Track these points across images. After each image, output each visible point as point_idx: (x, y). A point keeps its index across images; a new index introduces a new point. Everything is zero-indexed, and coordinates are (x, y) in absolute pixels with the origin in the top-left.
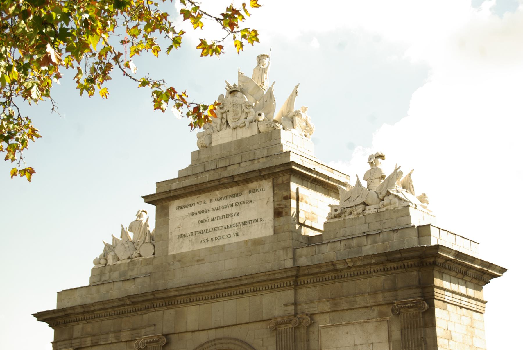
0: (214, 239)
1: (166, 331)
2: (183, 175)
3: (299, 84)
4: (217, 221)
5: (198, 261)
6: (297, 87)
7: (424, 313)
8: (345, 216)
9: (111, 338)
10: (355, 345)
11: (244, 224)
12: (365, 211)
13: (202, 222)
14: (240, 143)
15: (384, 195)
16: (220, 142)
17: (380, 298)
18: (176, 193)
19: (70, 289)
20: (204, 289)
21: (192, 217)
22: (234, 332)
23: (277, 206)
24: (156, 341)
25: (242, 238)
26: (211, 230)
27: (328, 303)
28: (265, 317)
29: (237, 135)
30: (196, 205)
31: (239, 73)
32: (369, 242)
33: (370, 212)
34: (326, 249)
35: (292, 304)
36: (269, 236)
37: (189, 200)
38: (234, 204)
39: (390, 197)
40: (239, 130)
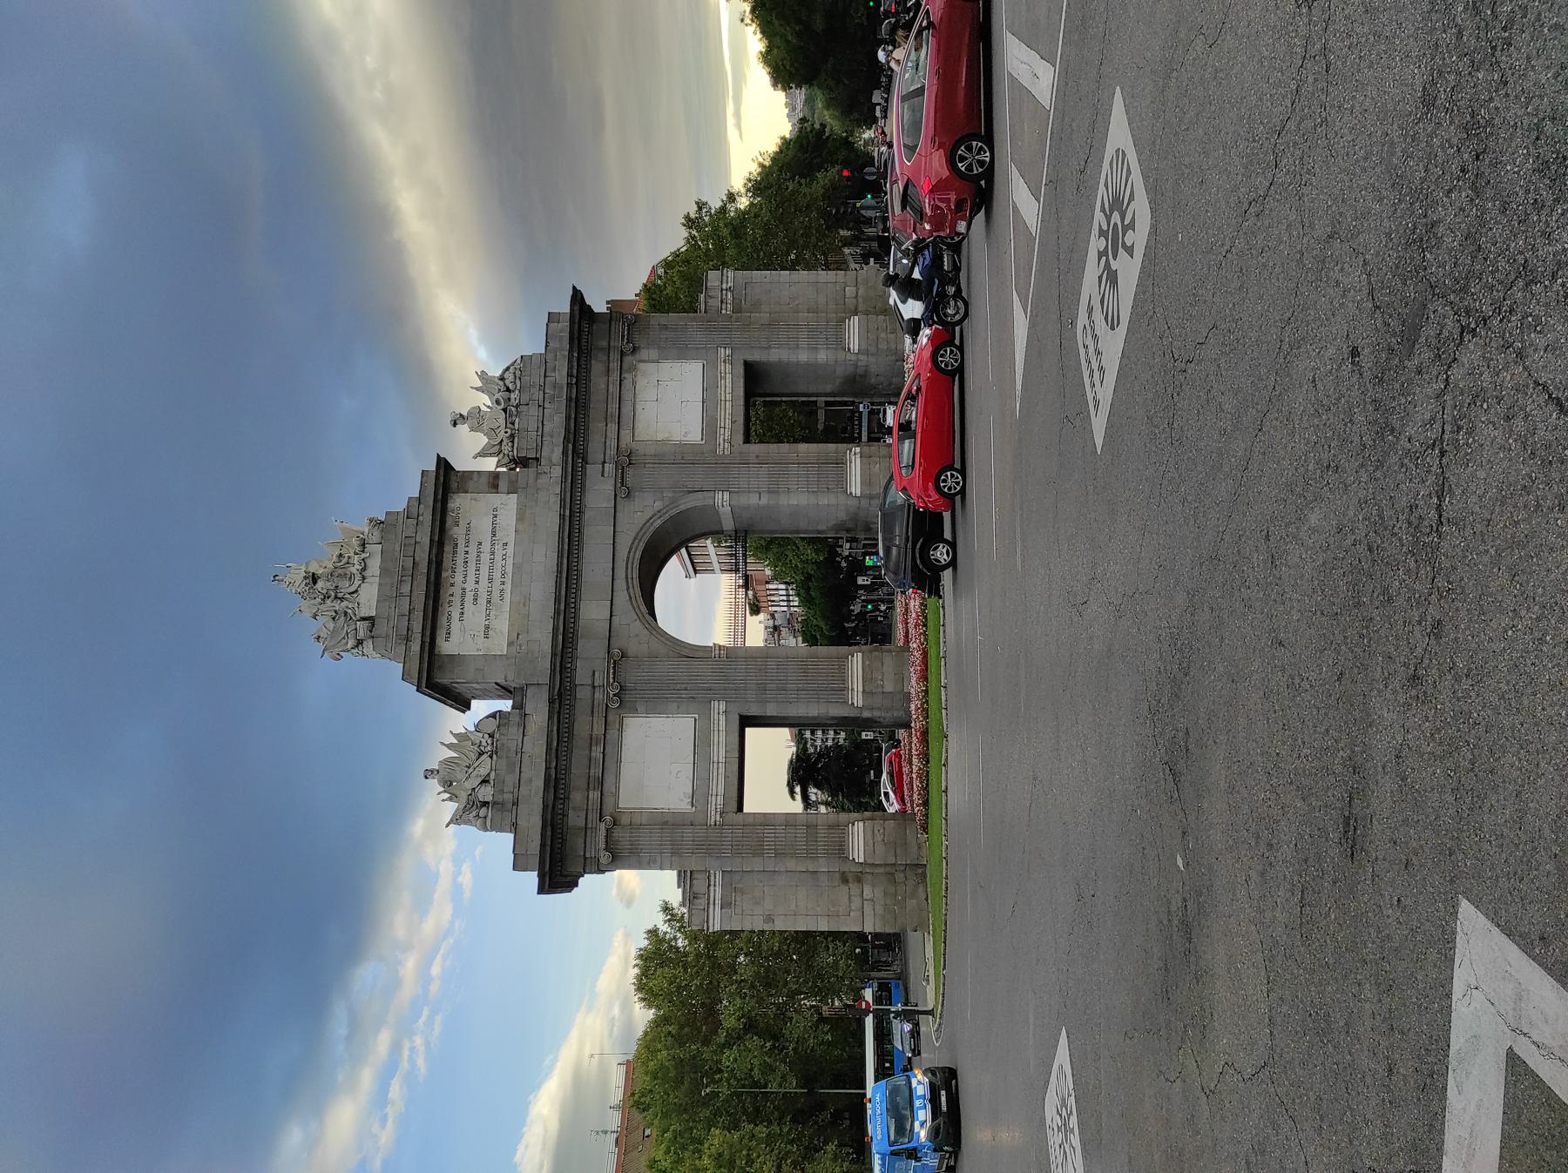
0: (502, 580)
5: (524, 605)
9: (597, 753)
14: (384, 571)
17: (615, 365)
18: (428, 633)
20: (564, 575)
24: (615, 661)
25: (511, 539)
26: (490, 585)
27: (609, 425)
32: (553, 375)
35: (603, 467)
37: (443, 621)
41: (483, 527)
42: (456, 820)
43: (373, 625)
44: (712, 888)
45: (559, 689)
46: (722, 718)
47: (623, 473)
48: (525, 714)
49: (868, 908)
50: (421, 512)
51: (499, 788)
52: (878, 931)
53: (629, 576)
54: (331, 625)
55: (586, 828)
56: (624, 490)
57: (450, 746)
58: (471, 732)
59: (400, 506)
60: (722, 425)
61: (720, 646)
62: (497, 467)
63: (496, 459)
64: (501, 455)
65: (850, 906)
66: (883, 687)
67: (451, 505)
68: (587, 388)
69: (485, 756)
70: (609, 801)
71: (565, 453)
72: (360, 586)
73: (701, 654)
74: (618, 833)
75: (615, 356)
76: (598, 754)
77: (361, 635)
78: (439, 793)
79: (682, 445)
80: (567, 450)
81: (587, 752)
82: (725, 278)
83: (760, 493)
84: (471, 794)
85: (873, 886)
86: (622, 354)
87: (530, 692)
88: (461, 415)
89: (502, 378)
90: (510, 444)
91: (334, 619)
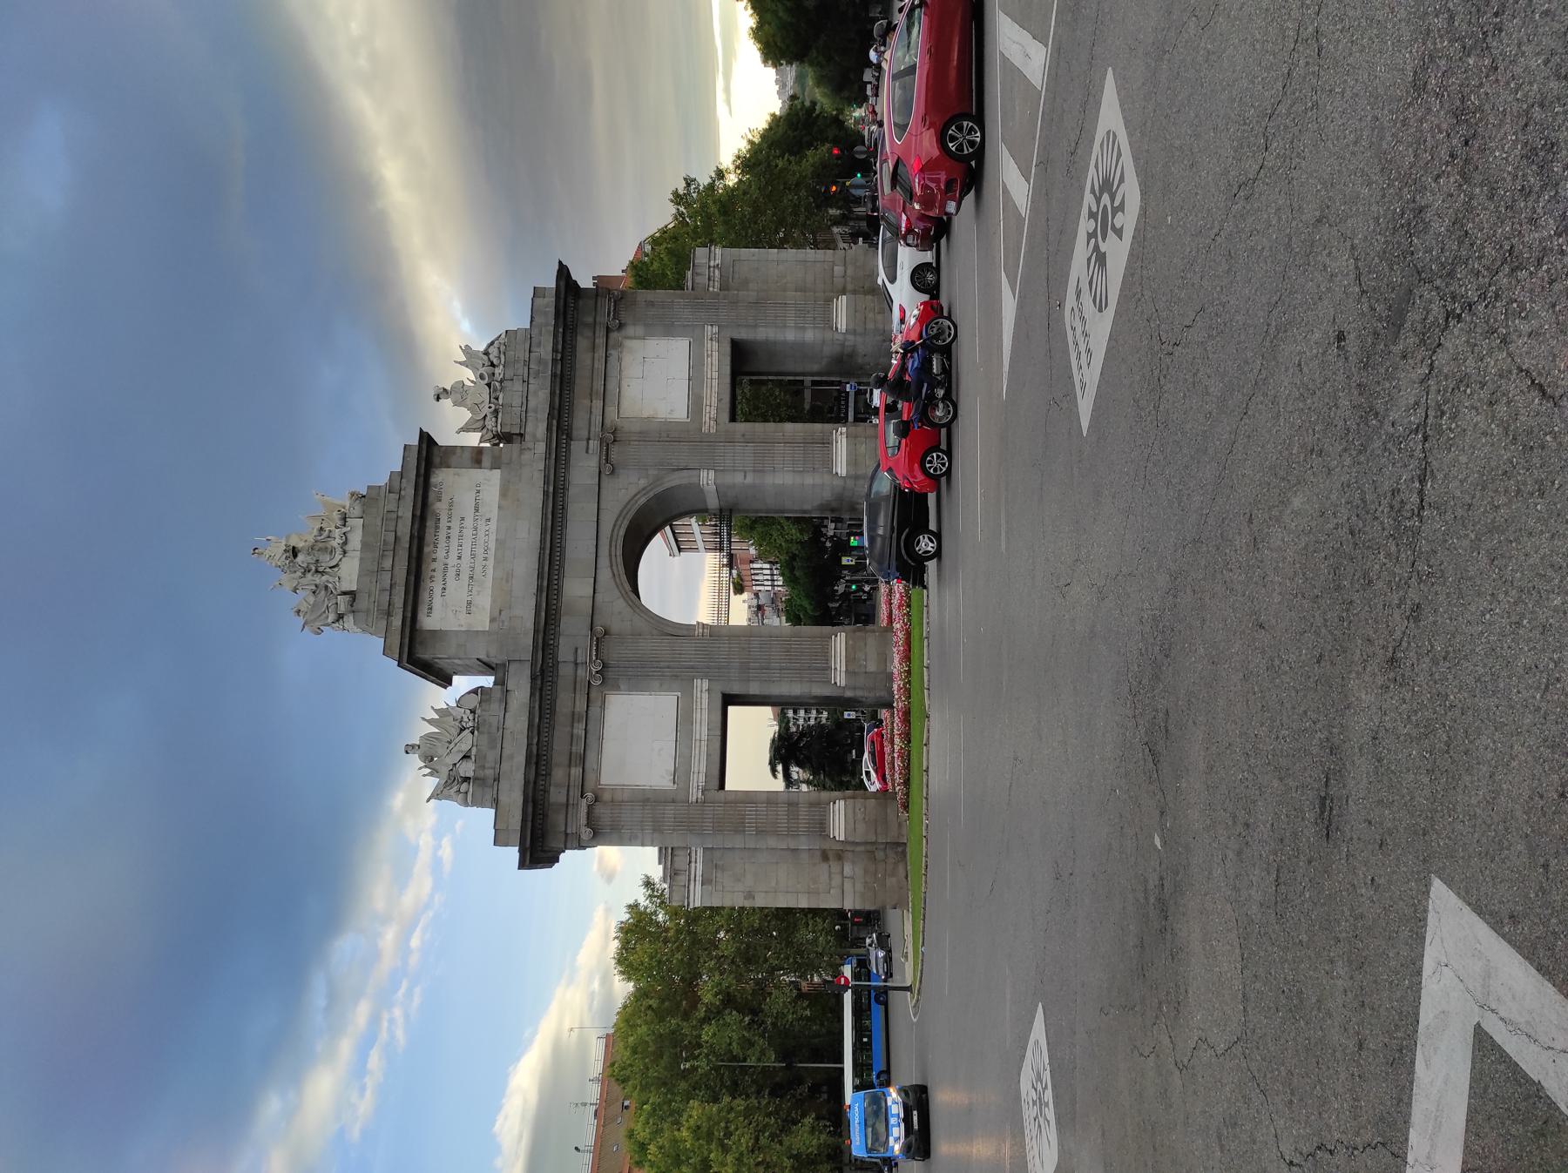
5: (507, 581)
9: (579, 730)
11: (477, 511)
14: (365, 545)
17: (600, 341)
18: (409, 608)
20: (548, 552)
24: (597, 638)
25: (494, 514)
27: (594, 401)
29: (354, 550)
34: (532, 404)
35: (588, 443)
37: (424, 596)
39: (490, 350)
41: (466, 501)
42: (437, 795)
43: (354, 600)
44: (693, 865)
45: (542, 665)
46: (705, 695)
47: (607, 449)
48: (507, 691)
49: (848, 886)
52: (858, 907)
53: (613, 554)
54: (312, 599)
55: (567, 805)
56: (608, 467)
57: (430, 722)
58: (453, 708)
59: (382, 480)
60: (708, 404)
61: (703, 624)
62: (481, 442)
63: (480, 434)
64: (485, 430)
65: (830, 884)
66: (865, 667)
67: (433, 480)
68: (573, 368)
69: (467, 731)
70: (590, 777)
71: (549, 428)
72: (340, 560)
73: (685, 633)
74: (599, 810)
75: (601, 333)
76: (580, 732)
77: (342, 609)
78: (420, 768)
79: (666, 423)
80: (552, 425)
81: (569, 729)
82: (712, 255)
83: (745, 472)
84: (452, 770)
85: (853, 863)
86: (608, 330)
87: (513, 668)
88: (445, 390)
89: (486, 353)
90: (494, 419)
91: (314, 592)
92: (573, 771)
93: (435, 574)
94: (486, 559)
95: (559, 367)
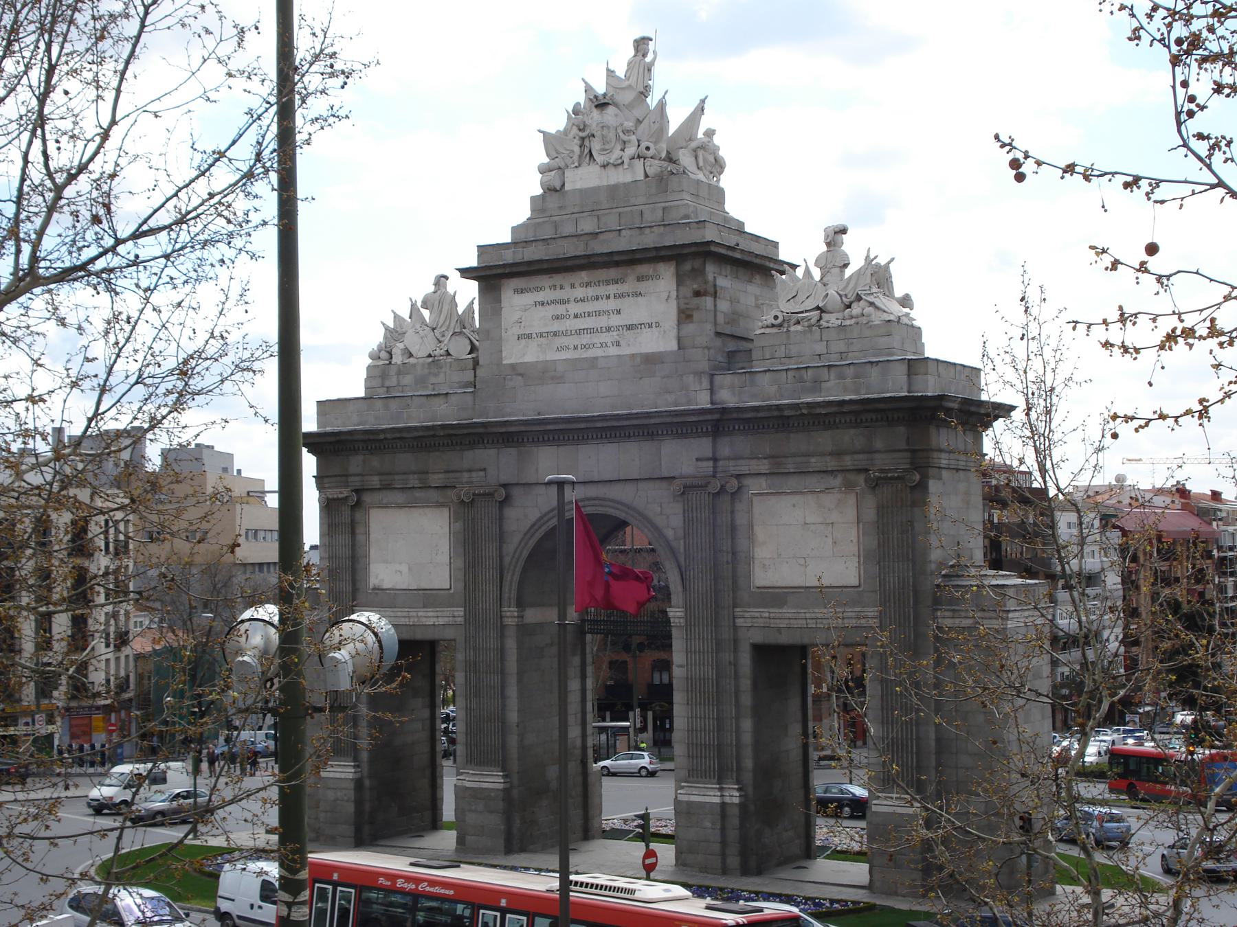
1: (504, 479)
2: (522, 236)
3: (706, 98)
4: (583, 319)
5: (553, 378)
6: (703, 101)
7: (913, 488)
8: (789, 326)
9: (414, 481)
10: (806, 524)
12: (821, 322)
13: (558, 317)
14: (613, 190)
15: (852, 299)
16: (578, 186)
17: (848, 461)
19: (339, 400)
21: (540, 308)
22: (616, 492)
23: (683, 306)
25: (626, 350)
27: (766, 461)
28: (667, 475)
30: (548, 290)
31: (608, 70)
32: (832, 376)
33: (830, 325)
35: (708, 459)
36: (671, 352)
38: (612, 296)
40: (611, 170)
41: (635, 311)
50: (655, 229)
51: (403, 369)
75: (860, 460)
79: (750, 560)
92: (376, 478)
93: (558, 289)
94: (576, 348)
95: (792, 413)
